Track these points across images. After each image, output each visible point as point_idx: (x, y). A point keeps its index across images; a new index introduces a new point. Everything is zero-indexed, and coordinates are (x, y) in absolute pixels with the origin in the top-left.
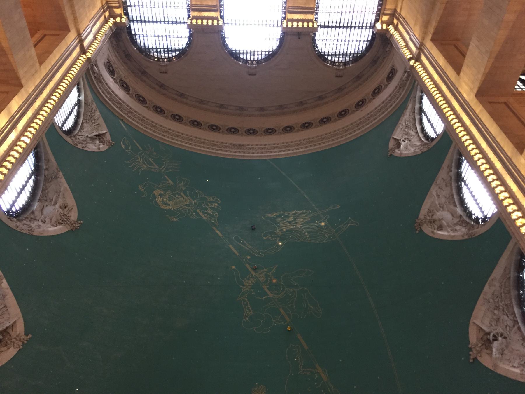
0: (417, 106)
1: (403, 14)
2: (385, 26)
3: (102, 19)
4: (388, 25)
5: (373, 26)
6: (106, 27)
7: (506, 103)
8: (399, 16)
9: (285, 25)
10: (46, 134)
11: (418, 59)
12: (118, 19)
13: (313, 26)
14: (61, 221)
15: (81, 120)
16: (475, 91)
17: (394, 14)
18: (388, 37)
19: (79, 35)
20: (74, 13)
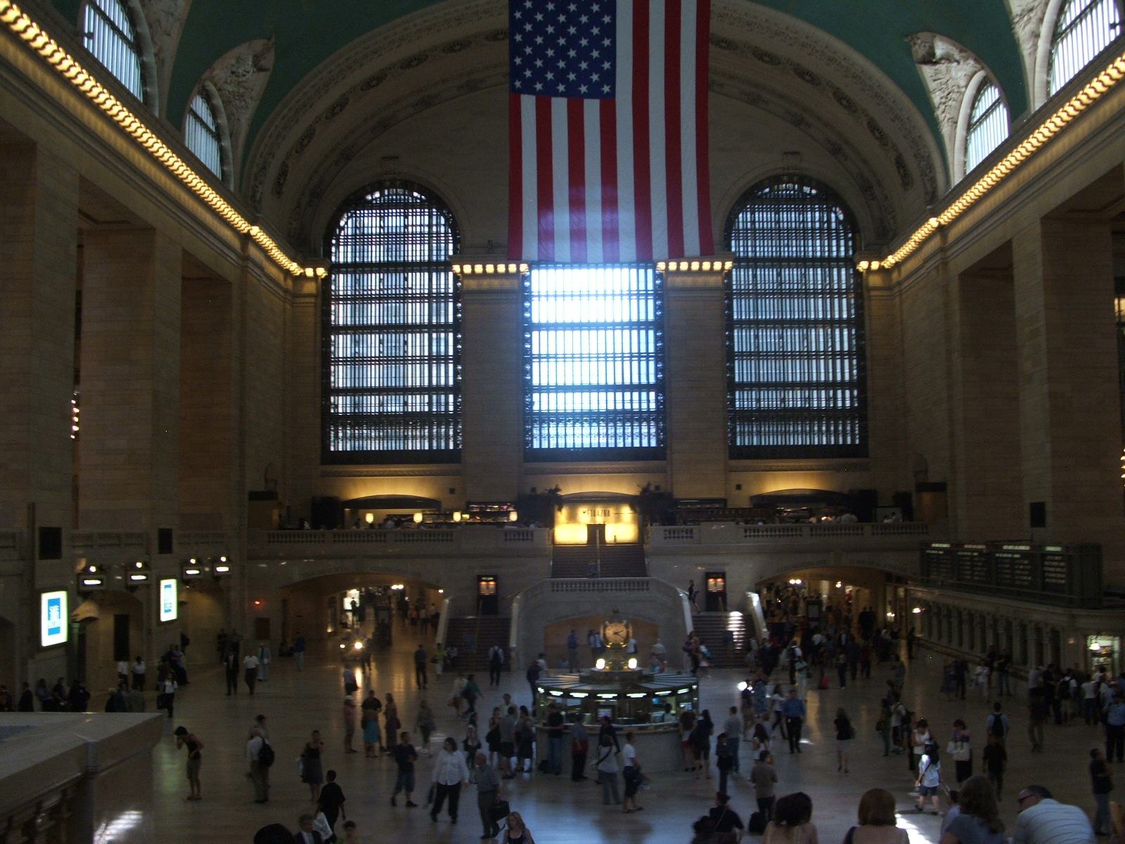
0: (226, 143)
1: (281, 303)
2: (309, 272)
5: (335, 268)
7: (95, 221)
8: (285, 298)
9: (524, 267)
11: (247, 238)
12: (875, 265)
13: (462, 268)
15: (970, 92)
19: (945, 263)
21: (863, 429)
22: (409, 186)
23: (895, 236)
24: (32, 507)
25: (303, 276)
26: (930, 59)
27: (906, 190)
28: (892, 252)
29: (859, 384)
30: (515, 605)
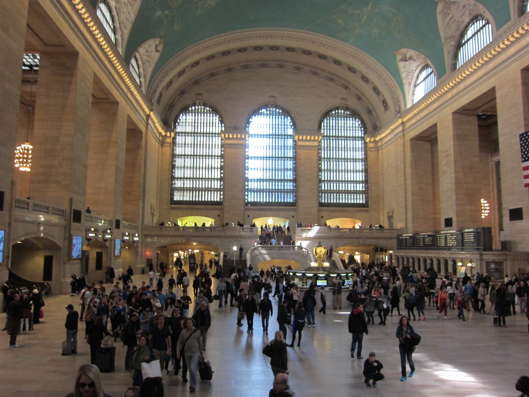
1: (157, 144)
2: (168, 134)
3: (385, 141)
4: (166, 135)
5: (176, 134)
6: (382, 136)
9: (247, 136)
10: (444, 73)
11: (148, 116)
12: (372, 140)
14: (452, 4)
16: (120, 107)
17: (162, 143)
18: (165, 127)
19: (404, 135)
20: (404, 151)
21: (367, 198)
22: (205, 105)
23: (380, 129)
24: (71, 200)
25: (166, 135)
26: (405, 59)
27: (386, 112)
28: (380, 134)
29: (366, 182)
30: (248, 256)
